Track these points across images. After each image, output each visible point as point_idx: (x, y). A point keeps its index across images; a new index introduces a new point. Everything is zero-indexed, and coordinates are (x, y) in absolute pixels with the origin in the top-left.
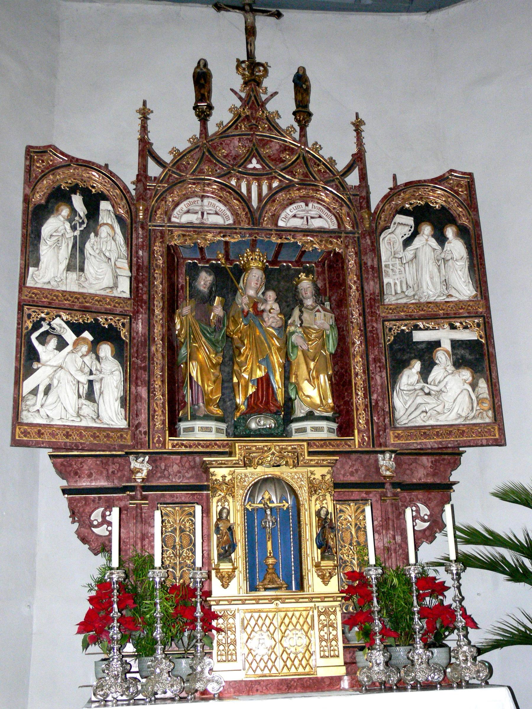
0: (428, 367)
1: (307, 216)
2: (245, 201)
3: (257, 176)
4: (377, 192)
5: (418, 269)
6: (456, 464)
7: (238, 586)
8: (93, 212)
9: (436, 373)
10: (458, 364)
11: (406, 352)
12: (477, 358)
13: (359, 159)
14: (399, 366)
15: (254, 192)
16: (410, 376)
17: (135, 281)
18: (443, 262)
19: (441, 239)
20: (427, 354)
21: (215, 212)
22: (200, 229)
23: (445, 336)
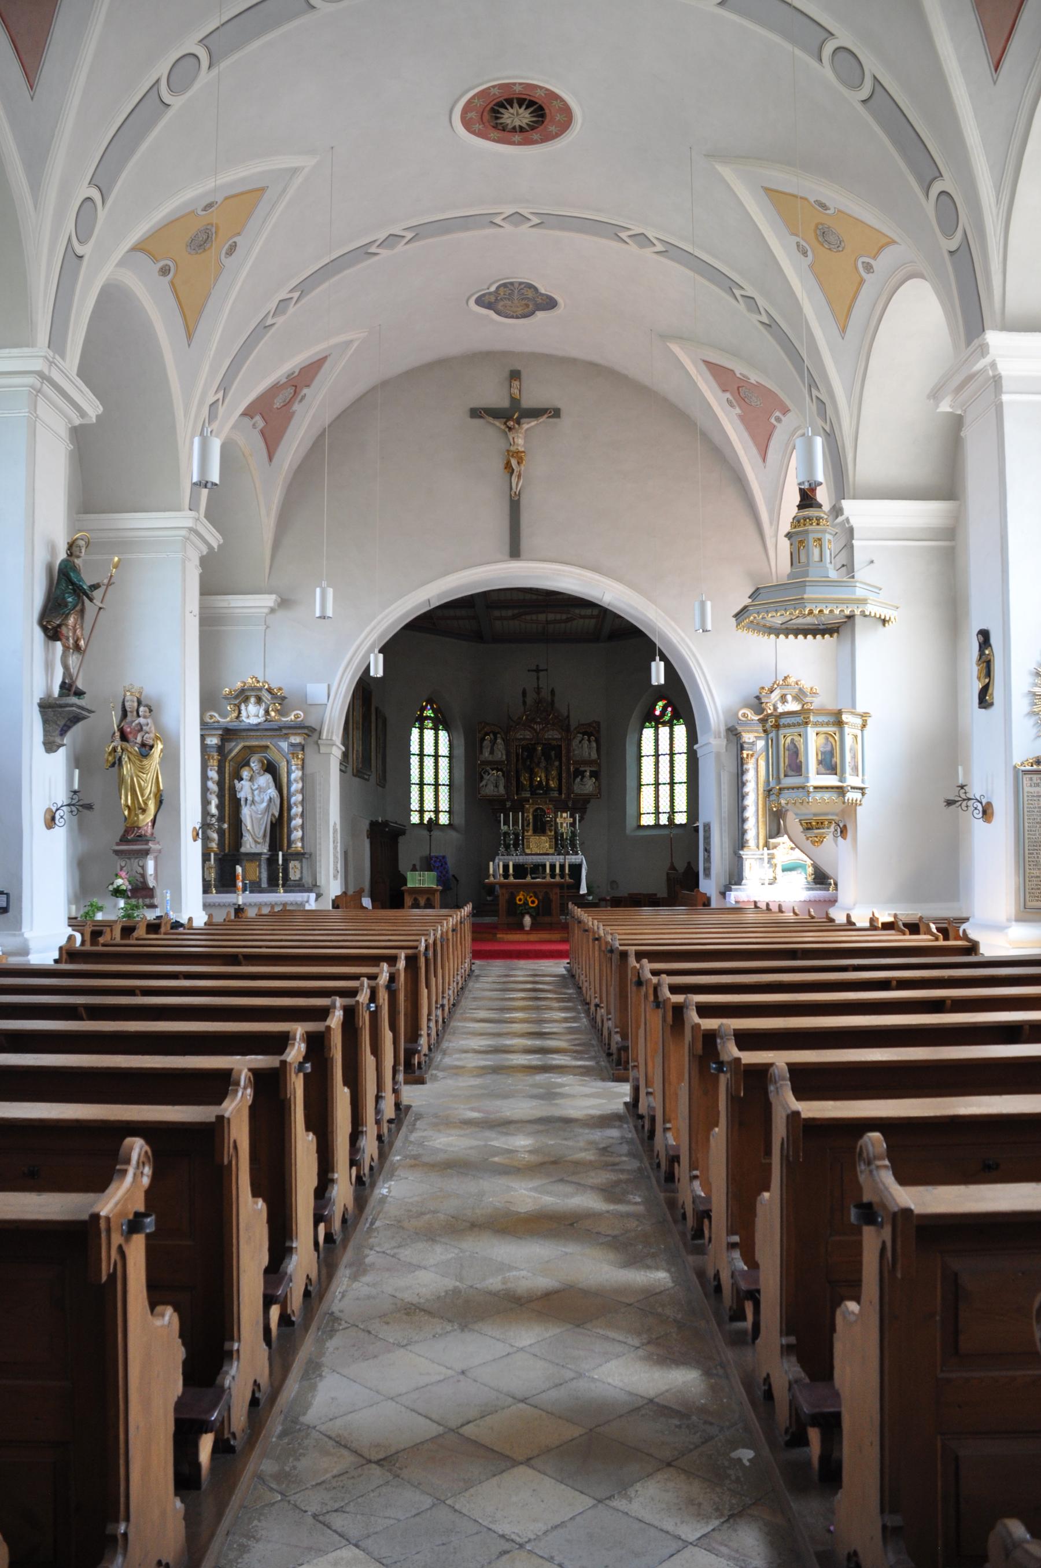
0: (583, 777)
1: (553, 735)
2: (535, 730)
3: (539, 723)
4: (573, 724)
5: (584, 749)
6: (589, 802)
7: (530, 833)
8: (496, 739)
9: (585, 780)
10: (591, 776)
11: (579, 773)
12: (595, 775)
13: (568, 717)
14: (575, 777)
15: (537, 727)
16: (578, 780)
17: (507, 755)
18: (590, 748)
19: (589, 741)
20: (582, 774)
21: (528, 735)
22: (524, 739)
23: (588, 769)
